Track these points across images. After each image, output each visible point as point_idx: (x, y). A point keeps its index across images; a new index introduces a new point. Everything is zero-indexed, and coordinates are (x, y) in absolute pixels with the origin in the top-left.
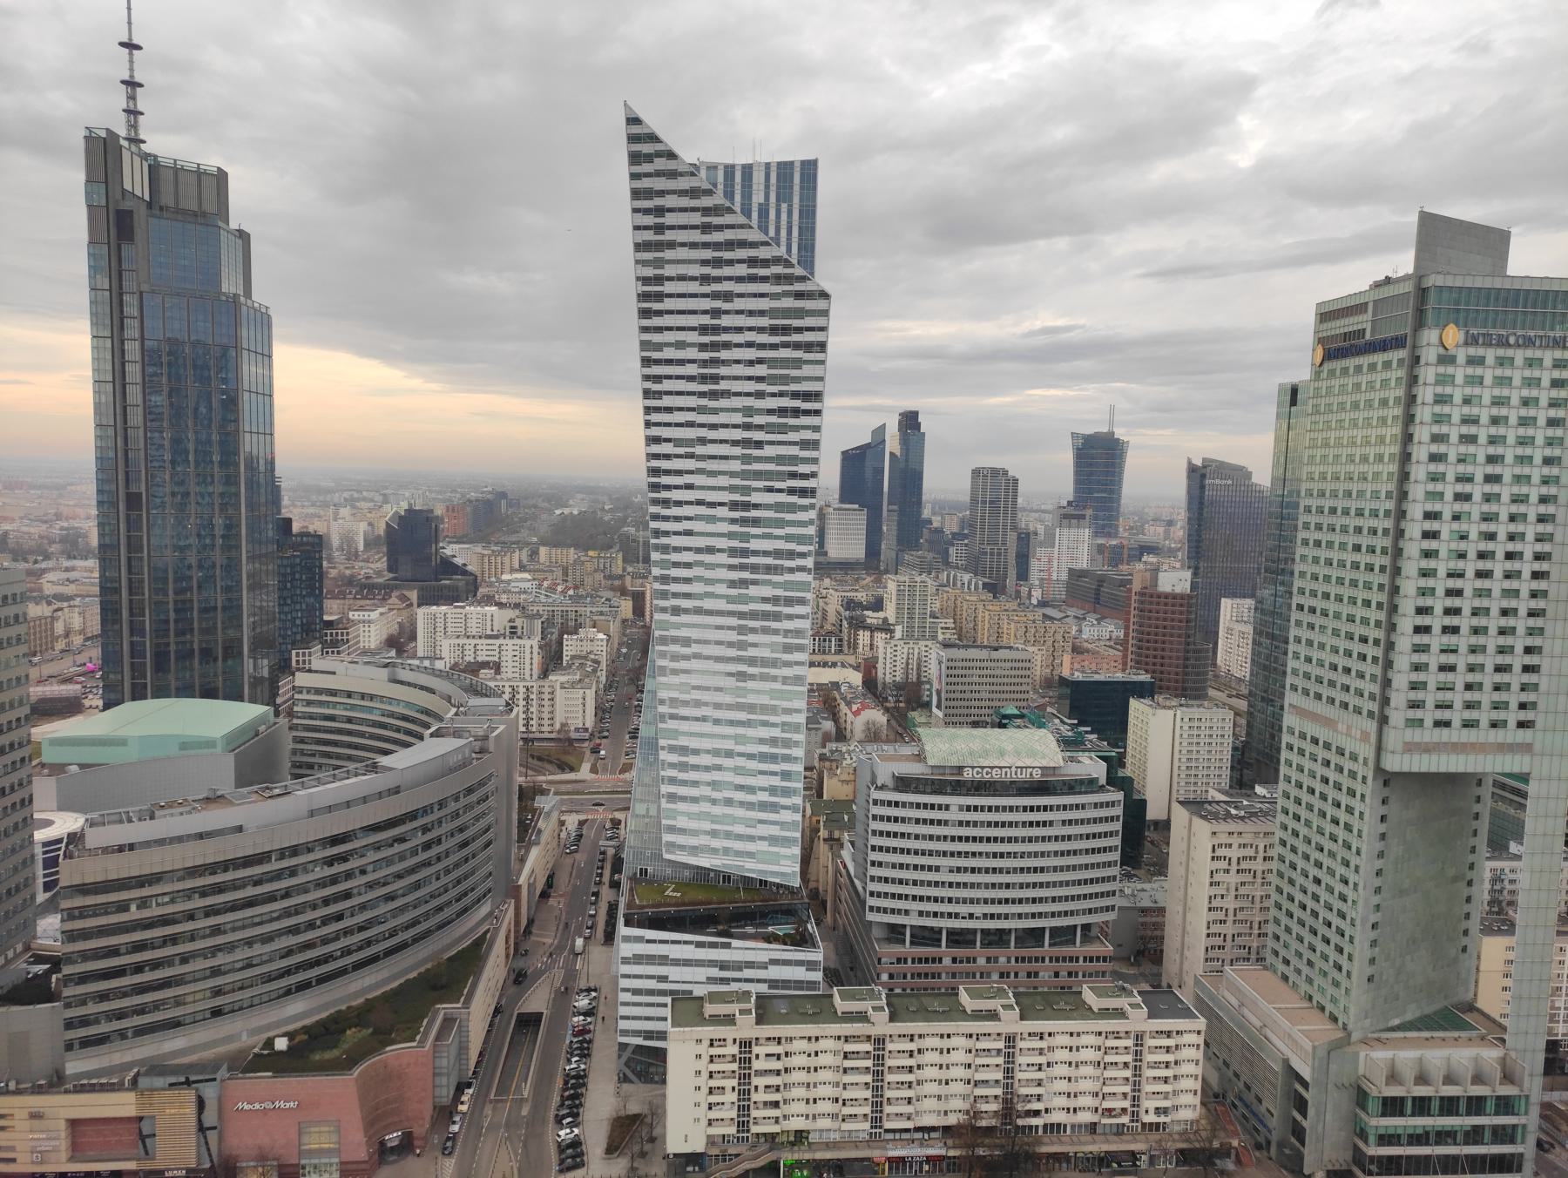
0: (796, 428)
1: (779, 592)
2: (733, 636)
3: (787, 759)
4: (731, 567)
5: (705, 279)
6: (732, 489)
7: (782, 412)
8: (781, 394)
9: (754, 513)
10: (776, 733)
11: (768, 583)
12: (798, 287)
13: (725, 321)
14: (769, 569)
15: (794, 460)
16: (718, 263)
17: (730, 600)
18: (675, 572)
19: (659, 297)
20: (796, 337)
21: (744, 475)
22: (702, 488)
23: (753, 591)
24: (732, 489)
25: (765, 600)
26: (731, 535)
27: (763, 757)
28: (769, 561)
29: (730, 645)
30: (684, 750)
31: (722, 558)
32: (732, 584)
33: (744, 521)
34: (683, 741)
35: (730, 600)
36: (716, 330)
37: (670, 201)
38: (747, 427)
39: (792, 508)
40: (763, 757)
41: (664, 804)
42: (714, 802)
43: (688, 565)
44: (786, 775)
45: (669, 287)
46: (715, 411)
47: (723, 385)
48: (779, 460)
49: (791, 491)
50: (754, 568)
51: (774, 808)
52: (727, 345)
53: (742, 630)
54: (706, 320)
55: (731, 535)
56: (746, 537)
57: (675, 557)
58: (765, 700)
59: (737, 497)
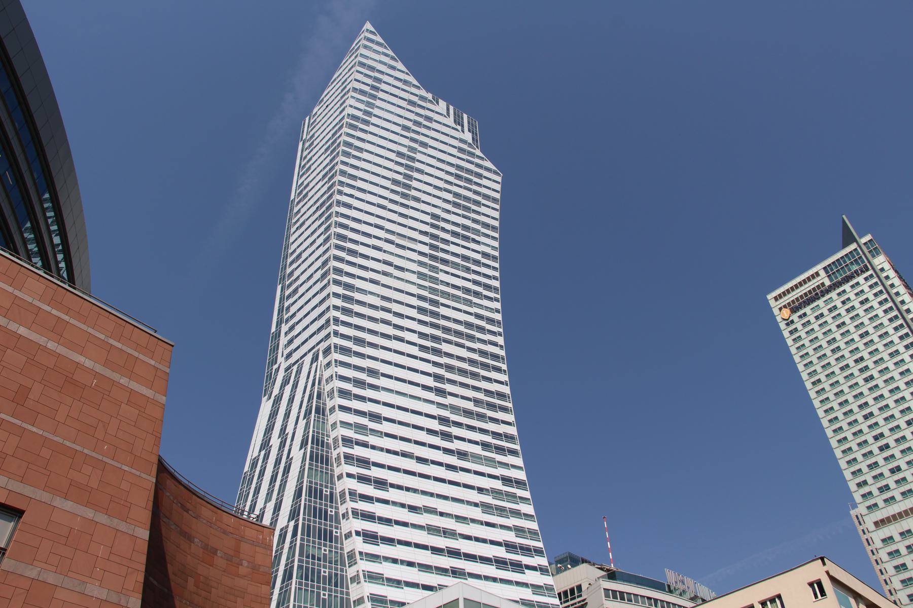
0: (478, 242)
1: (475, 356)
2: (430, 382)
3: (516, 513)
4: (421, 322)
5: (406, 128)
6: (421, 263)
7: (465, 228)
8: (464, 217)
9: (441, 287)
10: (498, 485)
11: (462, 346)
12: (477, 161)
13: (419, 156)
14: (458, 334)
15: (477, 262)
16: (416, 123)
17: (423, 348)
18: (357, 308)
19: (367, 123)
20: (474, 187)
21: (433, 258)
22: (392, 254)
23: (445, 347)
24: (421, 263)
25: (459, 358)
26: (421, 298)
27: (486, 508)
28: (461, 328)
29: (425, 388)
30: (381, 484)
31: (413, 313)
32: (422, 335)
33: (433, 291)
34: (375, 472)
35: (423, 348)
36: (413, 159)
37: (386, 78)
38: (433, 226)
39: (477, 294)
40: (486, 508)
41: (358, 544)
42: (436, 550)
43: (372, 306)
44: (519, 531)
45: (374, 120)
46: (406, 206)
47: (413, 193)
48: (465, 258)
49: (475, 282)
50: (446, 330)
51: (518, 567)
52: (421, 171)
53: (438, 378)
54: (404, 150)
55: (421, 298)
56: (435, 303)
57: (357, 296)
58: (477, 450)
59: (425, 271)
